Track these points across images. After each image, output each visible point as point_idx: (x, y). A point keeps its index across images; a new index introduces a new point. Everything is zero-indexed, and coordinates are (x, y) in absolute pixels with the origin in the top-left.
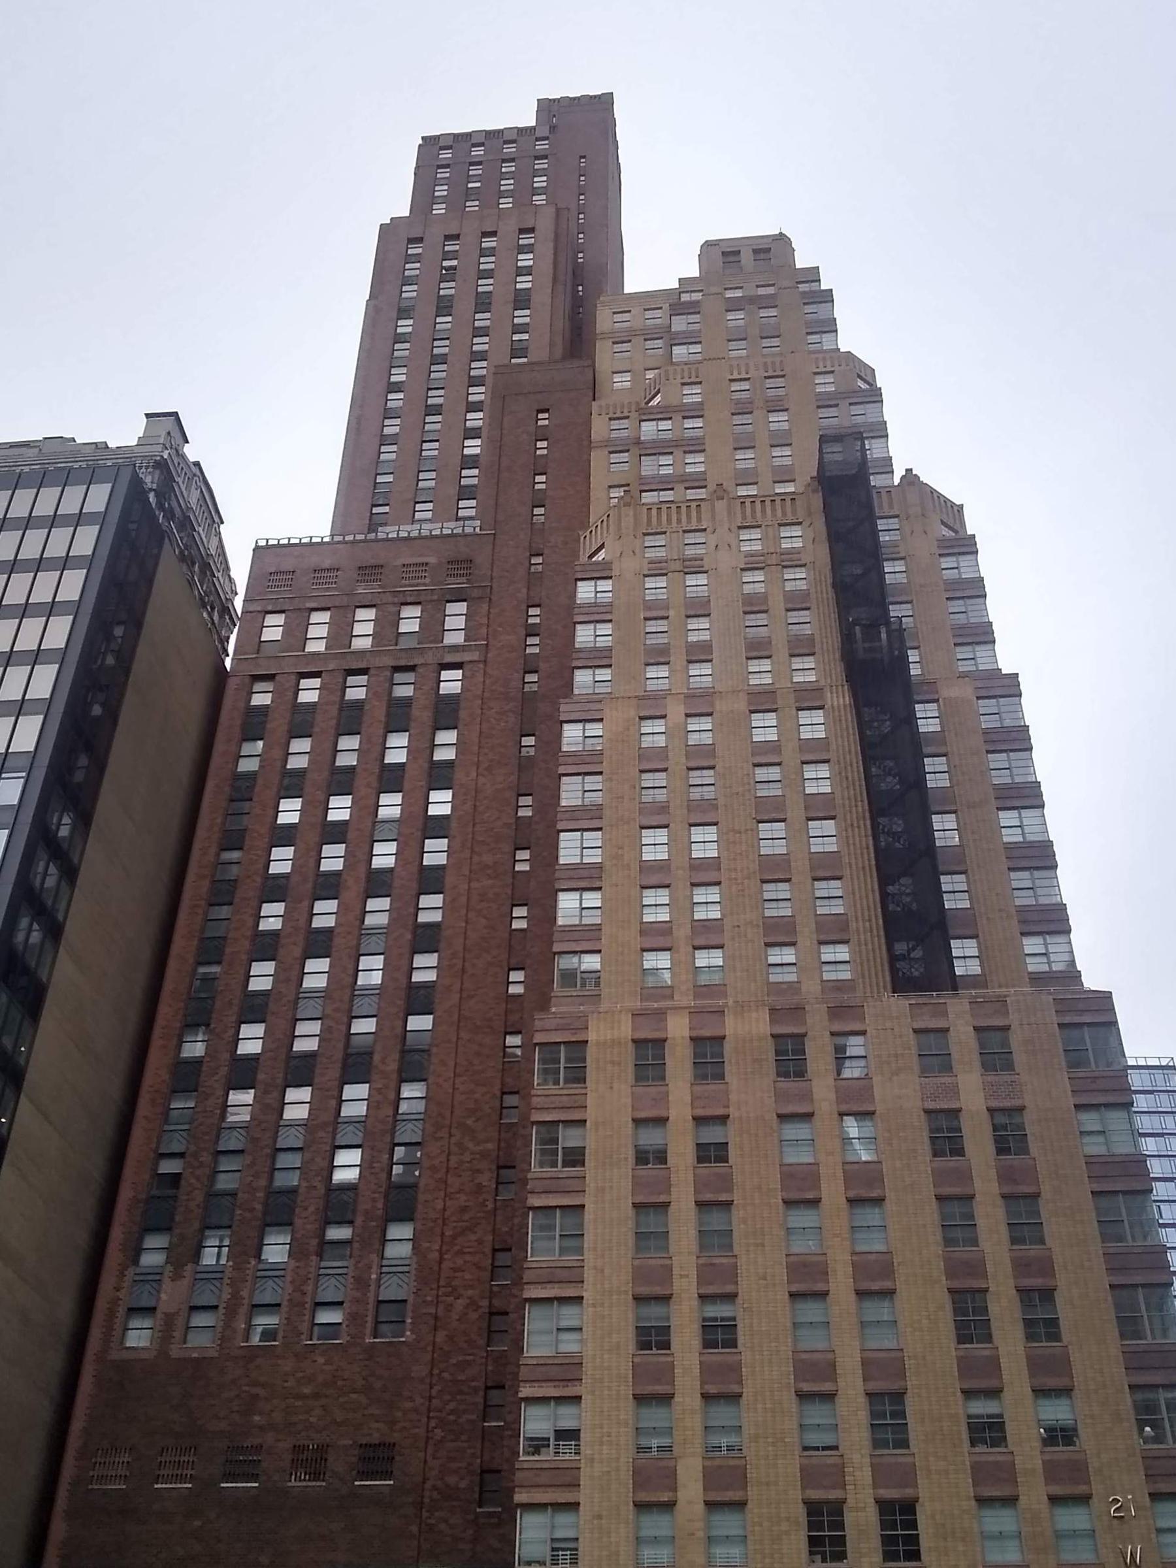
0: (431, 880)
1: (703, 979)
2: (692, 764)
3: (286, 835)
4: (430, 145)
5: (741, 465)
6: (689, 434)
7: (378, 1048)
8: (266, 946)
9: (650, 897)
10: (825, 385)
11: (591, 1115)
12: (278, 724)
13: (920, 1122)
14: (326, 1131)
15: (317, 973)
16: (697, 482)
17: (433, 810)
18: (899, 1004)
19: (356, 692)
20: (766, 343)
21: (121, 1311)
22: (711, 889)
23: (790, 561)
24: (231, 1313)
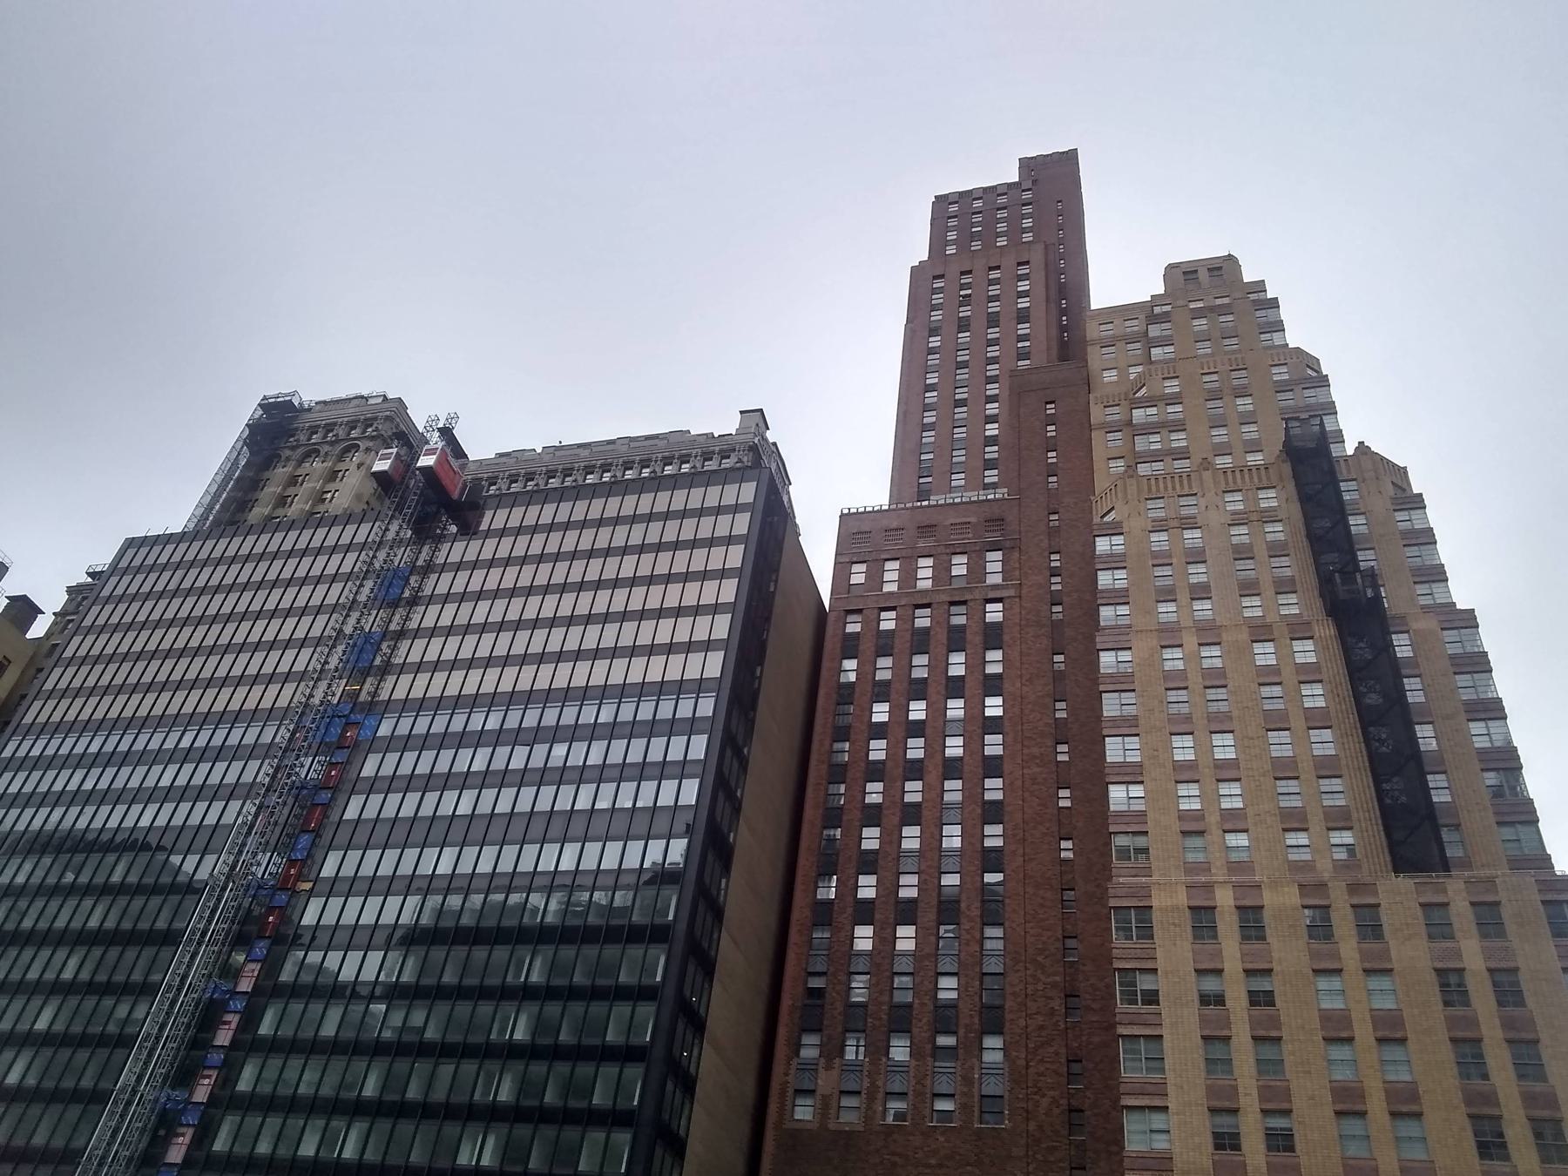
0: (992, 767)
1: (1234, 857)
2: (1208, 683)
3: (879, 731)
4: (940, 200)
5: (1217, 440)
6: (1171, 417)
7: (964, 897)
8: (873, 815)
9: (1183, 790)
10: (1281, 374)
11: (1160, 964)
12: (867, 646)
13: (1432, 977)
14: (926, 962)
15: (911, 838)
16: (1182, 454)
17: (989, 712)
18: (1405, 883)
19: (923, 622)
20: (1227, 342)
21: (790, 1092)
22: (1234, 785)
23: (1268, 517)
24: (871, 1098)
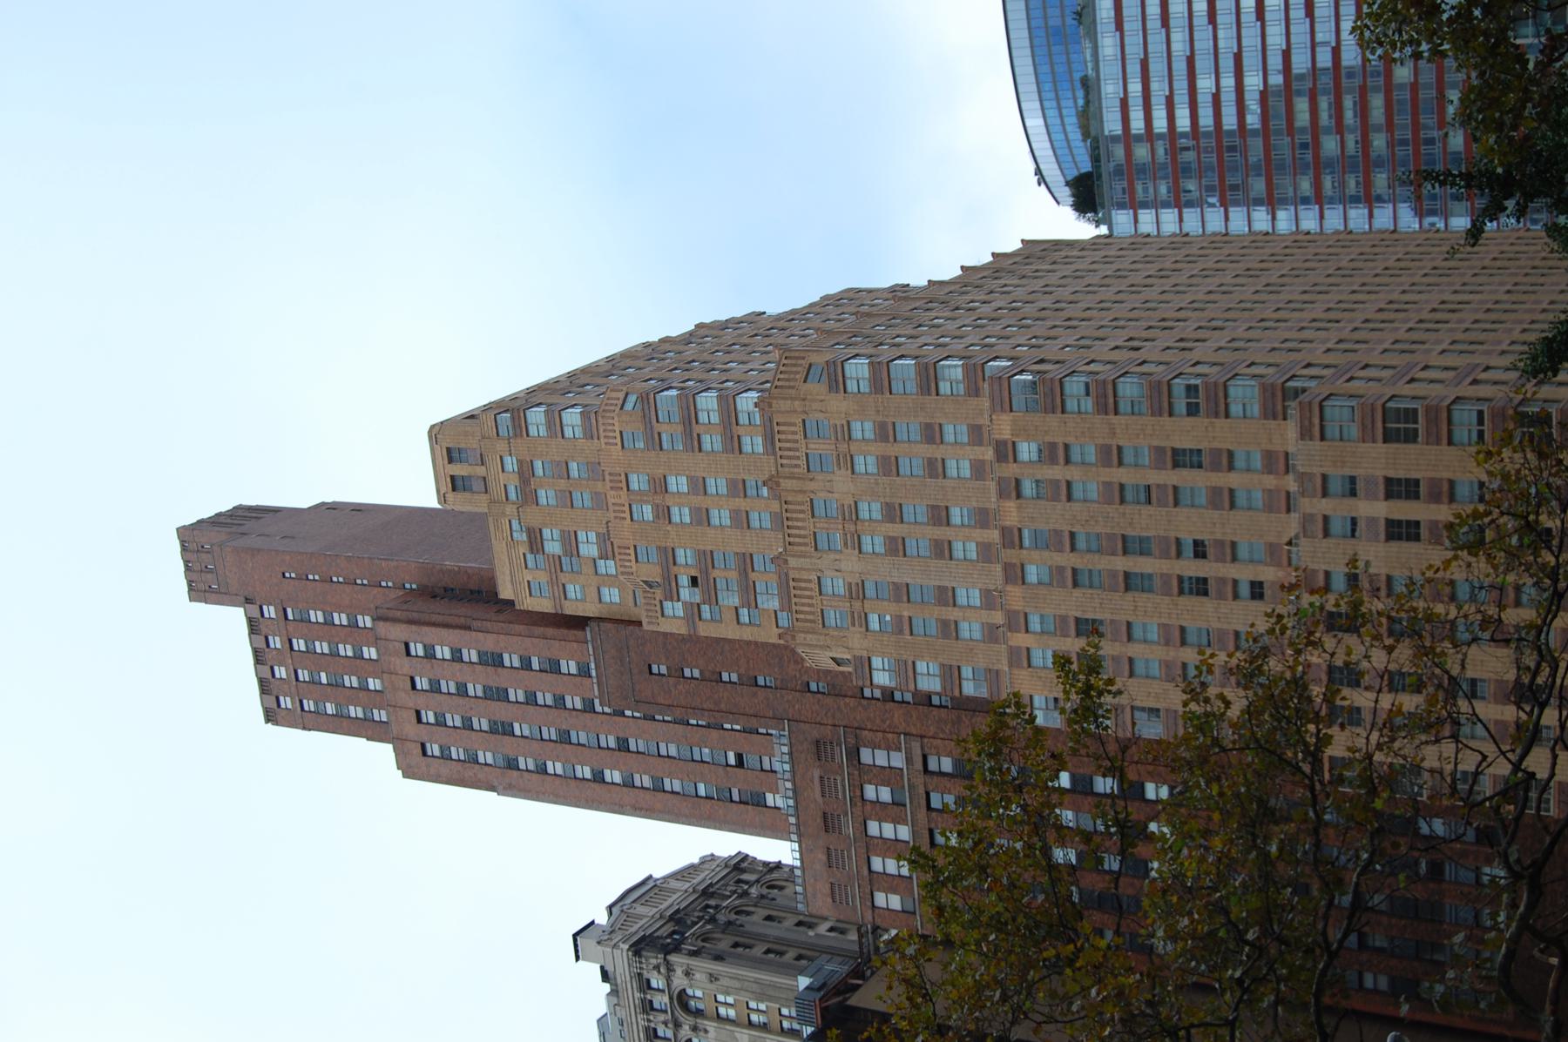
4: (272, 716)
